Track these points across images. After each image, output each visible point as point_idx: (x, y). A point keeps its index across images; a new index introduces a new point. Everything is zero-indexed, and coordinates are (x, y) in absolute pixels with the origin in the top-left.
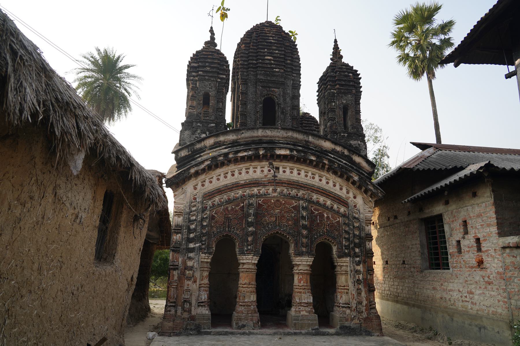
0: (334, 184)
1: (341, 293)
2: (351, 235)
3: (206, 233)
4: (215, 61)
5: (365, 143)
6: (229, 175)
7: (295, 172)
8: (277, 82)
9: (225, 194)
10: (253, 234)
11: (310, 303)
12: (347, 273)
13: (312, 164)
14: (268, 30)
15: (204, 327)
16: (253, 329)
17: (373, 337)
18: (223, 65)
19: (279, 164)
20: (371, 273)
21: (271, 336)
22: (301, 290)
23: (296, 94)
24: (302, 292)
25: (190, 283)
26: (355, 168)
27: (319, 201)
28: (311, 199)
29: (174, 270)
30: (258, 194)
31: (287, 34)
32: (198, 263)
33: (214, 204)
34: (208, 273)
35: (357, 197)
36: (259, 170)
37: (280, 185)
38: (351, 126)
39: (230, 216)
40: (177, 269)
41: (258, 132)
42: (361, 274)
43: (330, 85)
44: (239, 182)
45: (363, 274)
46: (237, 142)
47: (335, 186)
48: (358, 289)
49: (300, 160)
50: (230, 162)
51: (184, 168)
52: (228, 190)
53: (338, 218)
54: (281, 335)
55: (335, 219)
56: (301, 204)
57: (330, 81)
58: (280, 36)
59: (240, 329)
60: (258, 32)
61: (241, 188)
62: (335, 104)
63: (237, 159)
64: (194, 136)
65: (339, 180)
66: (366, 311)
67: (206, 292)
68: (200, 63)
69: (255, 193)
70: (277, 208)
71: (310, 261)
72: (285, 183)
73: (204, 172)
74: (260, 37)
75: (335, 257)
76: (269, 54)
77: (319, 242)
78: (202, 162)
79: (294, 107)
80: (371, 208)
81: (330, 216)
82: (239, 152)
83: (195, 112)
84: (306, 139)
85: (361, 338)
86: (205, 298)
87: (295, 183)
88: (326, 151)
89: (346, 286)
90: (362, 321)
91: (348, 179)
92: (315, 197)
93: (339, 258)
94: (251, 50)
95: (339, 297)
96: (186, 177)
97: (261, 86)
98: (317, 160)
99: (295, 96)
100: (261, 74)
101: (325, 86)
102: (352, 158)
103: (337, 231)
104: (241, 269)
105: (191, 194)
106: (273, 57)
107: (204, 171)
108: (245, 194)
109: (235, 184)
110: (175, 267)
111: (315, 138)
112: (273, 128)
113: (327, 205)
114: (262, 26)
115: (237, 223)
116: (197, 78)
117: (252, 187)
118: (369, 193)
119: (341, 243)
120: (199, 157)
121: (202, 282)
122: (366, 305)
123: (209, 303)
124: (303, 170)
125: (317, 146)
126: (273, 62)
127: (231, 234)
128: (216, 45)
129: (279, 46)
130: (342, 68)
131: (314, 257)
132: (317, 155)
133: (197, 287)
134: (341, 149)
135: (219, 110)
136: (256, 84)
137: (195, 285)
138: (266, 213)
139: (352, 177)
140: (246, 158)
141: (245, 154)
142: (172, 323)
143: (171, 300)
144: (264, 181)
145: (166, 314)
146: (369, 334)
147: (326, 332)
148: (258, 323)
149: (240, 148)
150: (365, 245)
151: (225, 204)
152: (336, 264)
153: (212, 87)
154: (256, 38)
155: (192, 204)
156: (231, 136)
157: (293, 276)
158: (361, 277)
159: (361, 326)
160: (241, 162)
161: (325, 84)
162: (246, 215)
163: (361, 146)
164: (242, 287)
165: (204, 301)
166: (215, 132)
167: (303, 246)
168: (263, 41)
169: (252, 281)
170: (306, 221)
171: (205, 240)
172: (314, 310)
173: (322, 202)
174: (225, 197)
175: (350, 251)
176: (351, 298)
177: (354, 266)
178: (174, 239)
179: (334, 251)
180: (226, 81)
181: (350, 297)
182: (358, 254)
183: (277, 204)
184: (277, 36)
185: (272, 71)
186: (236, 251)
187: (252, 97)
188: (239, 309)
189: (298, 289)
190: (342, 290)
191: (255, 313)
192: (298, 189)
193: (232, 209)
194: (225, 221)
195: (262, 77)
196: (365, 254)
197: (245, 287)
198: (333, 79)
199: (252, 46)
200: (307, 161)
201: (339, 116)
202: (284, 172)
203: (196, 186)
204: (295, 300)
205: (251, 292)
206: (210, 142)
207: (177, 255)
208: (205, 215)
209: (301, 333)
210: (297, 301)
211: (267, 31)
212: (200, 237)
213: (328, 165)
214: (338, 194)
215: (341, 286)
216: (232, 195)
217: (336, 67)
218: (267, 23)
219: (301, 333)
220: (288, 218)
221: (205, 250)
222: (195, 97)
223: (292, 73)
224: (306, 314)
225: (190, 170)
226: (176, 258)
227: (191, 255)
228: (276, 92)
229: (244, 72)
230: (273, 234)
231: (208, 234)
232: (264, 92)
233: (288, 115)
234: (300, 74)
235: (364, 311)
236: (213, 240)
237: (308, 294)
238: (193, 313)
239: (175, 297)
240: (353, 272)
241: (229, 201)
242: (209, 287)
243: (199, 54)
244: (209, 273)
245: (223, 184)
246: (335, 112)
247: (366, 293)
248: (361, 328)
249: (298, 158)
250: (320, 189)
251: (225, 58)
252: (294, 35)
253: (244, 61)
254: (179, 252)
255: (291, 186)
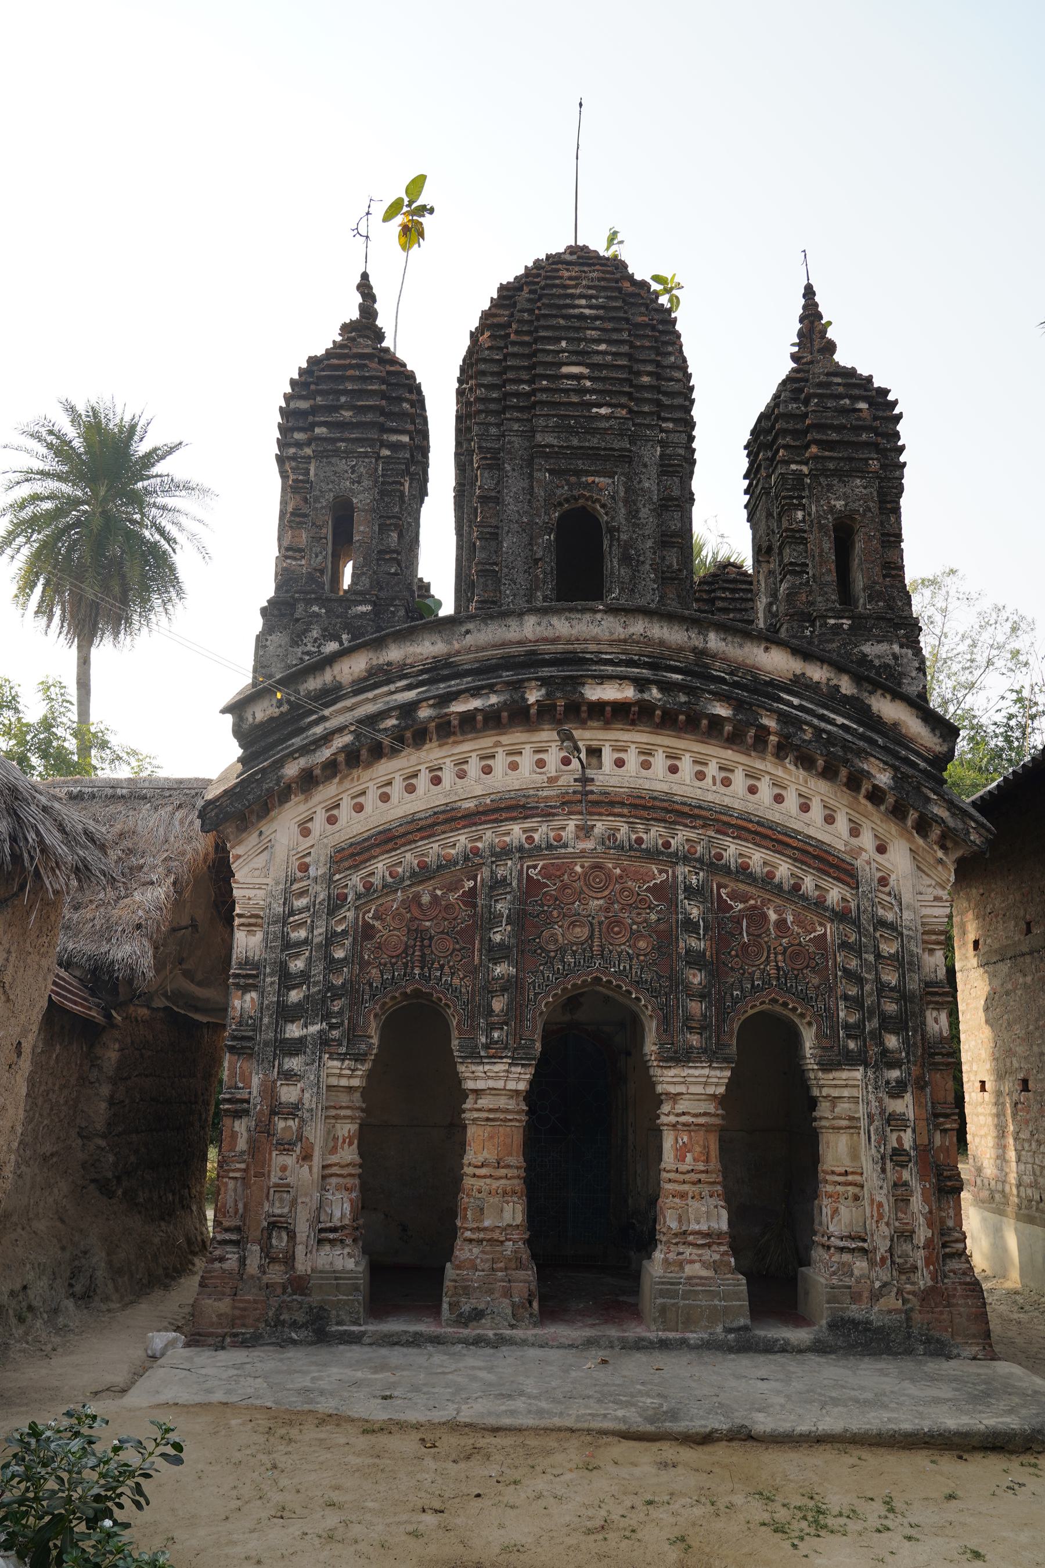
0: (803, 800)
1: (835, 1197)
2: (867, 988)
3: (343, 984)
4: (369, 387)
5: (918, 651)
6: (423, 782)
7: (659, 762)
8: (602, 453)
9: (408, 847)
10: (509, 985)
11: (720, 1234)
12: (855, 1123)
13: (721, 732)
14: (574, 274)
15: (338, 1316)
16: (512, 1327)
17: (953, 1363)
18: (400, 399)
19: (601, 735)
20: (948, 1126)
21: (574, 1351)
22: (686, 1187)
23: (676, 493)
24: (690, 1194)
25: (290, 1160)
26: (880, 741)
27: (748, 866)
28: (720, 857)
29: (234, 1117)
30: (527, 846)
31: (644, 284)
32: (315, 1090)
33: (372, 884)
34: (357, 1126)
35: (890, 848)
36: (526, 761)
37: (603, 810)
38: (864, 590)
39: (428, 924)
40: (246, 1112)
41: (522, 624)
42: (909, 1131)
43: (786, 447)
44: (459, 804)
45: (914, 1131)
46: (448, 665)
47: (805, 808)
48: (895, 1185)
49: (676, 720)
50: (420, 737)
51: (266, 760)
52: (419, 835)
53: (821, 924)
54: (612, 1347)
55: (809, 928)
56: (680, 878)
57: (784, 432)
58: (617, 294)
59: (466, 1325)
60: (538, 283)
61: (464, 827)
62: (804, 516)
63: (449, 722)
64: (300, 650)
65: (820, 789)
66: (927, 1266)
67: (345, 1194)
68: (319, 399)
69: (516, 843)
70: (594, 895)
71: (716, 1080)
72: (622, 804)
73: (334, 776)
74: (545, 301)
75: (810, 1067)
76: (574, 358)
77: (751, 1012)
78: (326, 739)
79: (667, 539)
80: (944, 888)
81: (790, 919)
82: (455, 699)
83: (303, 566)
84: (697, 643)
85: (908, 1365)
86: (343, 1216)
87: (657, 803)
88: (771, 683)
89: (853, 1173)
90: (914, 1301)
91: (854, 783)
92: (732, 850)
93: (823, 1070)
94: (511, 349)
95: (826, 1211)
96: (270, 792)
97: (547, 470)
98: (734, 715)
99: (672, 499)
100: (546, 426)
101: (770, 454)
102: (869, 706)
103: (814, 972)
104: (471, 1110)
105: (294, 852)
106: (587, 366)
107: (331, 768)
108: (479, 845)
109: (444, 812)
110: (238, 1106)
111: (730, 638)
112: (578, 611)
113: (777, 880)
114: (554, 263)
115: (454, 950)
116: (308, 451)
117: (502, 821)
118: (936, 832)
119: (831, 1015)
120: (316, 722)
121: (334, 1159)
122: (929, 1244)
123: (358, 1233)
124: (688, 755)
125: (738, 669)
126: (588, 384)
127: (433, 988)
128: (380, 336)
129: (609, 325)
130: (828, 385)
131: (732, 1069)
132: (737, 699)
133: (315, 1176)
134: (828, 675)
135: (387, 557)
136: (530, 463)
137: (306, 1167)
138: (555, 913)
139: (868, 775)
140: (480, 718)
141: (476, 703)
142: (228, 1300)
143: (226, 1223)
144: (546, 797)
145: (210, 1272)
146: (940, 1350)
147: (777, 1340)
148: (530, 1303)
149: (458, 685)
150: (924, 1023)
151: (408, 882)
152: (816, 1092)
153: (360, 476)
154: (528, 306)
155: (294, 887)
156: (427, 643)
157: (657, 1133)
158: (907, 1139)
159: (908, 1319)
160: (463, 732)
161: (769, 446)
162: (482, 920)
163: (905, 660)
164: (474, 1175)
165: (339, 1224)
166: (372, 634)
167: (689, 1028)
168: (554, 312)
169: (510, 1154)
170: (699, 939)
171: (340, 1013)
172: (732, 1260)
173: (758, 870)
174: (410, 858)
175: (865, 1045)
176: (872, 1216)
177: (880, 1100)
178: (234, 1008)
179: (808, 1045)
180: (412, 455)
181: (868, 1214)
182: (897, 1055)
183: (594, 880)
184: (602, 294)
185: (585, 417)
186: (452, 1051)
187: (518, 511)
188: (463, 1252)
189: (675, 1181)
190: (838, 1187)
191: (520, 1266)
192: (671, 823)
193: (435, 897)
194: (411, 942)
195: (550, 439)
196: (923, 1054)
197: (485, 1177)
198: (798, 426)
199: (517, 332)
200: (699, 722)
201: (821, 556)
202: (620, 763)
203: (309, 825)
204: (665, 1222)
205: (505, 1193)
206: (355, 667)
207: (245, 1065)
208: (340, 922)
209: (683, 1343)
210: (669, 1228)
211: (570, 278)
212: (324, 1000)
213: (776, 734)
214: (820, 836)
215: (833, 1173)
216: (433, 849)
217: (807, 381)
218: (571, 253)
219: (683, 1343)
220: (635, 927)
221: (340, 1045)
222: (305, 516)
223: (659, 418)
224: (704, 1273)
225: (282, 766)
226: (242, 1074)
227: (294, 1063)
228: (601, 490)
229: (491, 424)
230: (580, 987)
231: (351, 991)
232: (559, 492)
233: (648, 567)
234: (692, 425)
235: (920, 1263)
236: (370, 1011)
237: (713, 1202)
238: (302, 1265)
239: (241, 1211)
240: (876, 1123)
241: (424, 873)
242: (360, 1176)
243: (315, 368)
244: (361, 1125)
245: (399, 812)
246: (806, 544)
247: (926, 1200)
248: (911, 1327)
249: (666, 713)
250: (751, 821)
251: (411, 376)
252: (672, 289)
253: (489, 387)
254: (251, 1055)
255: (645, 814)
